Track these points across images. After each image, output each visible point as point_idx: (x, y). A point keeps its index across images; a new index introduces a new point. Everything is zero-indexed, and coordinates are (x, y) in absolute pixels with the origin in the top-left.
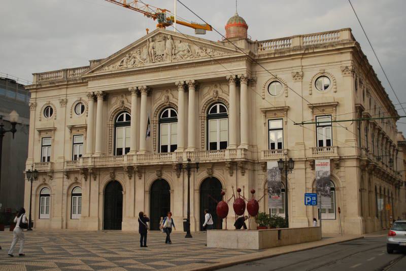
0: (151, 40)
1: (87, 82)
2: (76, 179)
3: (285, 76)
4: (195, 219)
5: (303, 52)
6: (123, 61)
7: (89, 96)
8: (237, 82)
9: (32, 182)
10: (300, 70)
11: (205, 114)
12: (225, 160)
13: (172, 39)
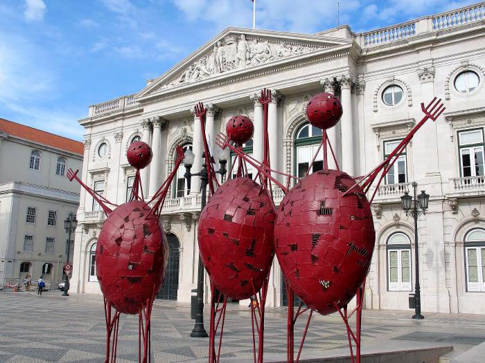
0: (219, 44)
1: (142, 110)
4: (275, 290)
5: (434, 38)
6: (184, 76)
7: (143, 124)
9: (70, 234)
10: (428, 66)
11: (292, 138)
13: (246, 40)
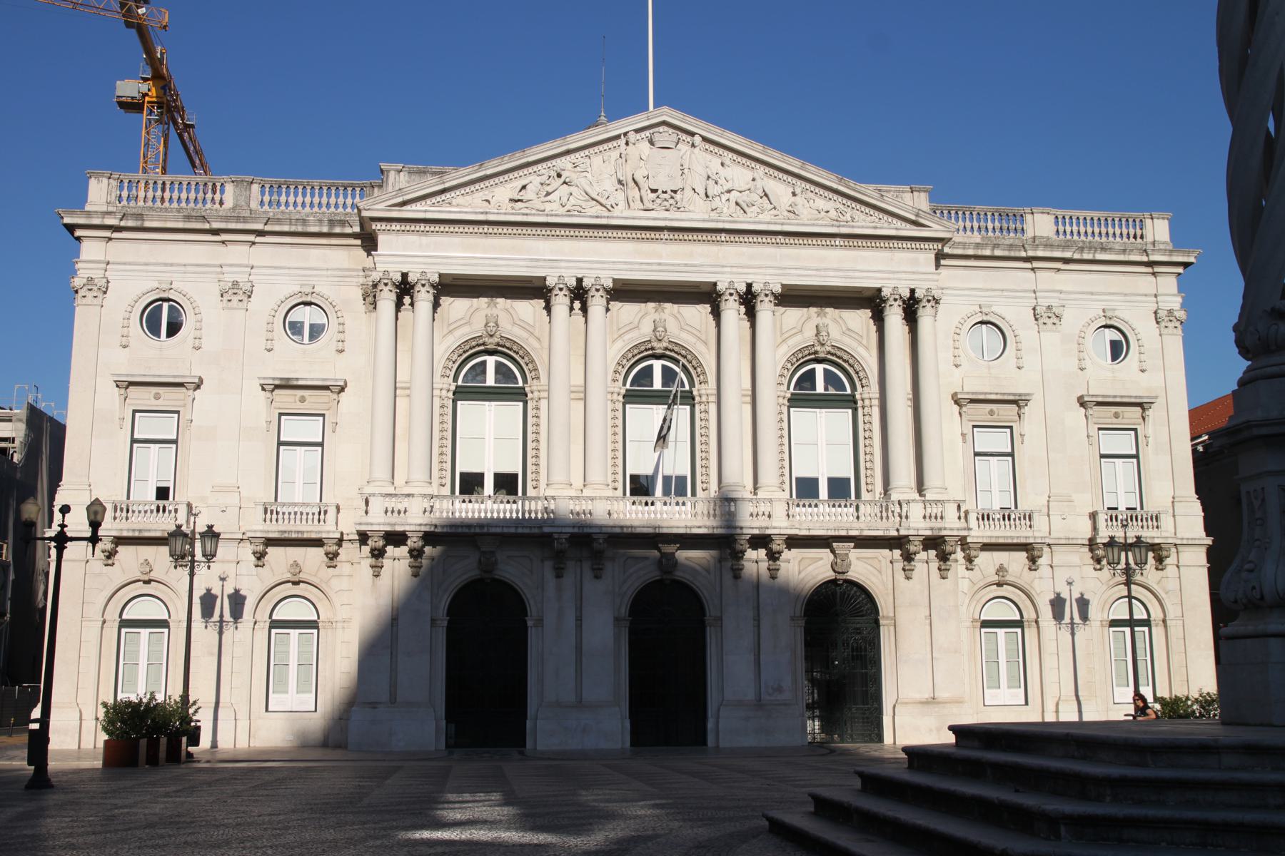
3: (1015, 314)
8: (911, 309)
10: (1054, 302)
12: (911, 532)
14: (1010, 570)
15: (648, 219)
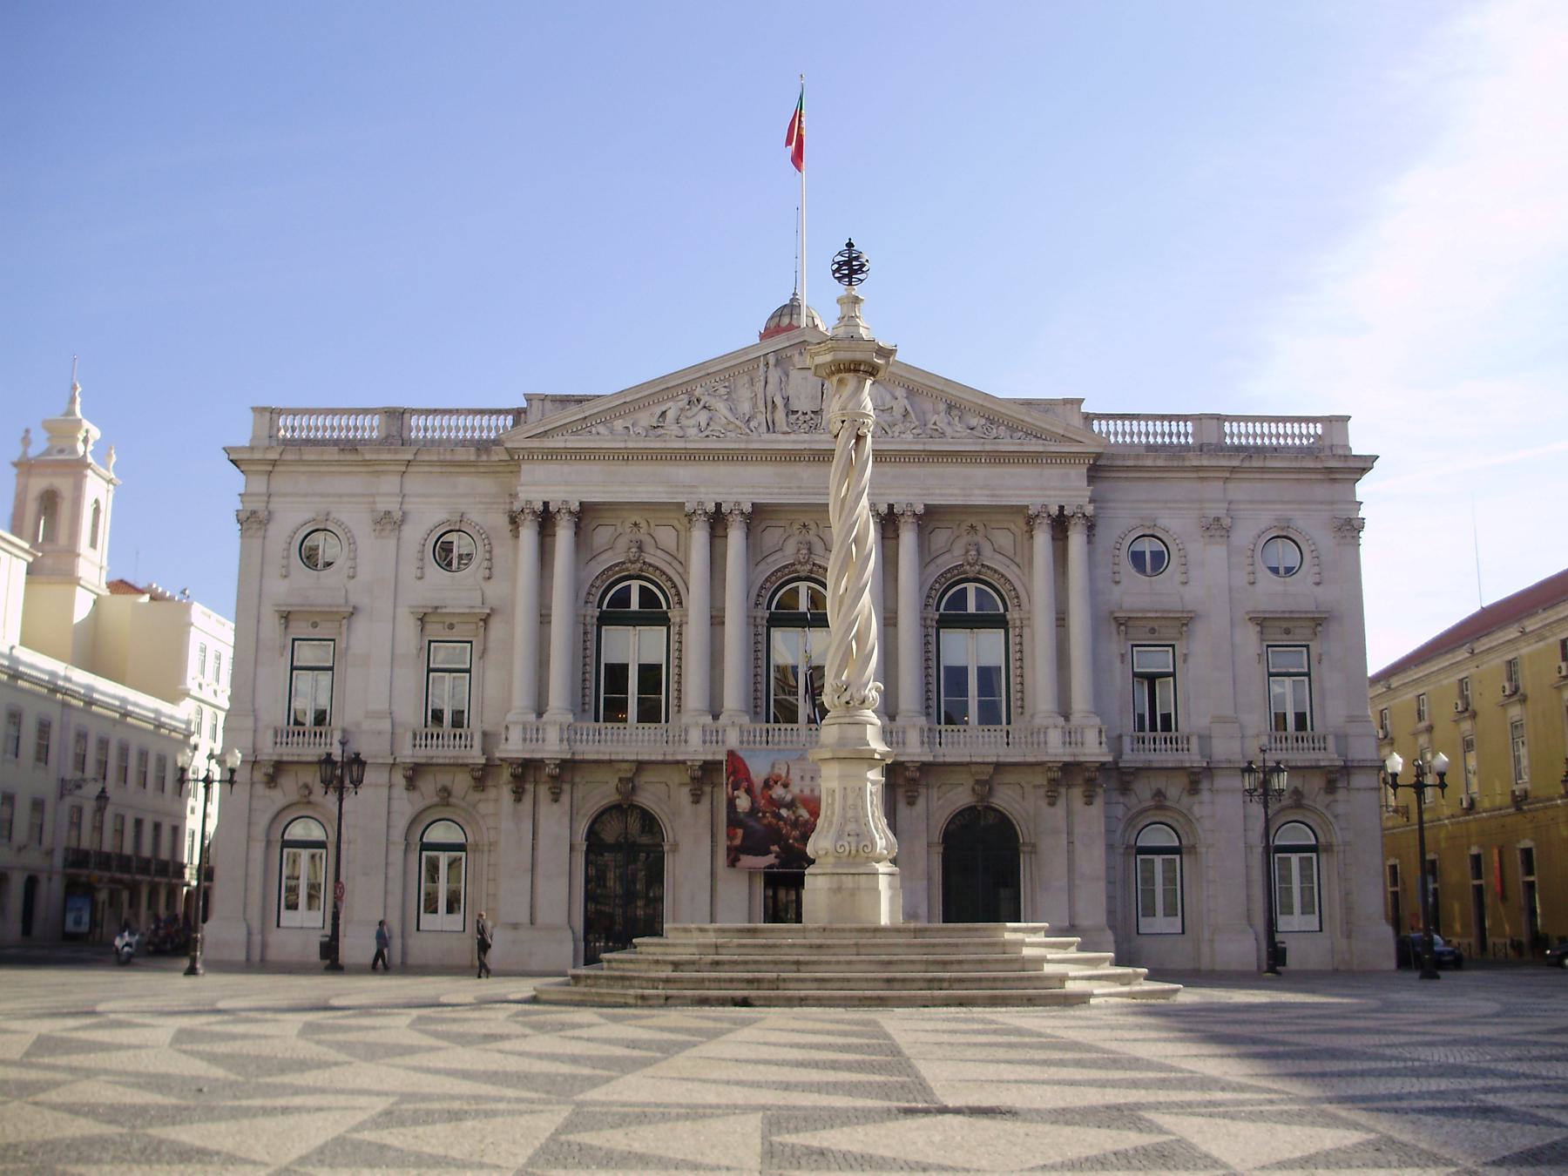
0: (772, 360)
2: (446, 792)
5: (1236, 463)
6: (664, 413)
8: (1060, 525)
9: (341, 800)
10: (1221, 513)
14: (1168, 794)
15: (787, 442)
